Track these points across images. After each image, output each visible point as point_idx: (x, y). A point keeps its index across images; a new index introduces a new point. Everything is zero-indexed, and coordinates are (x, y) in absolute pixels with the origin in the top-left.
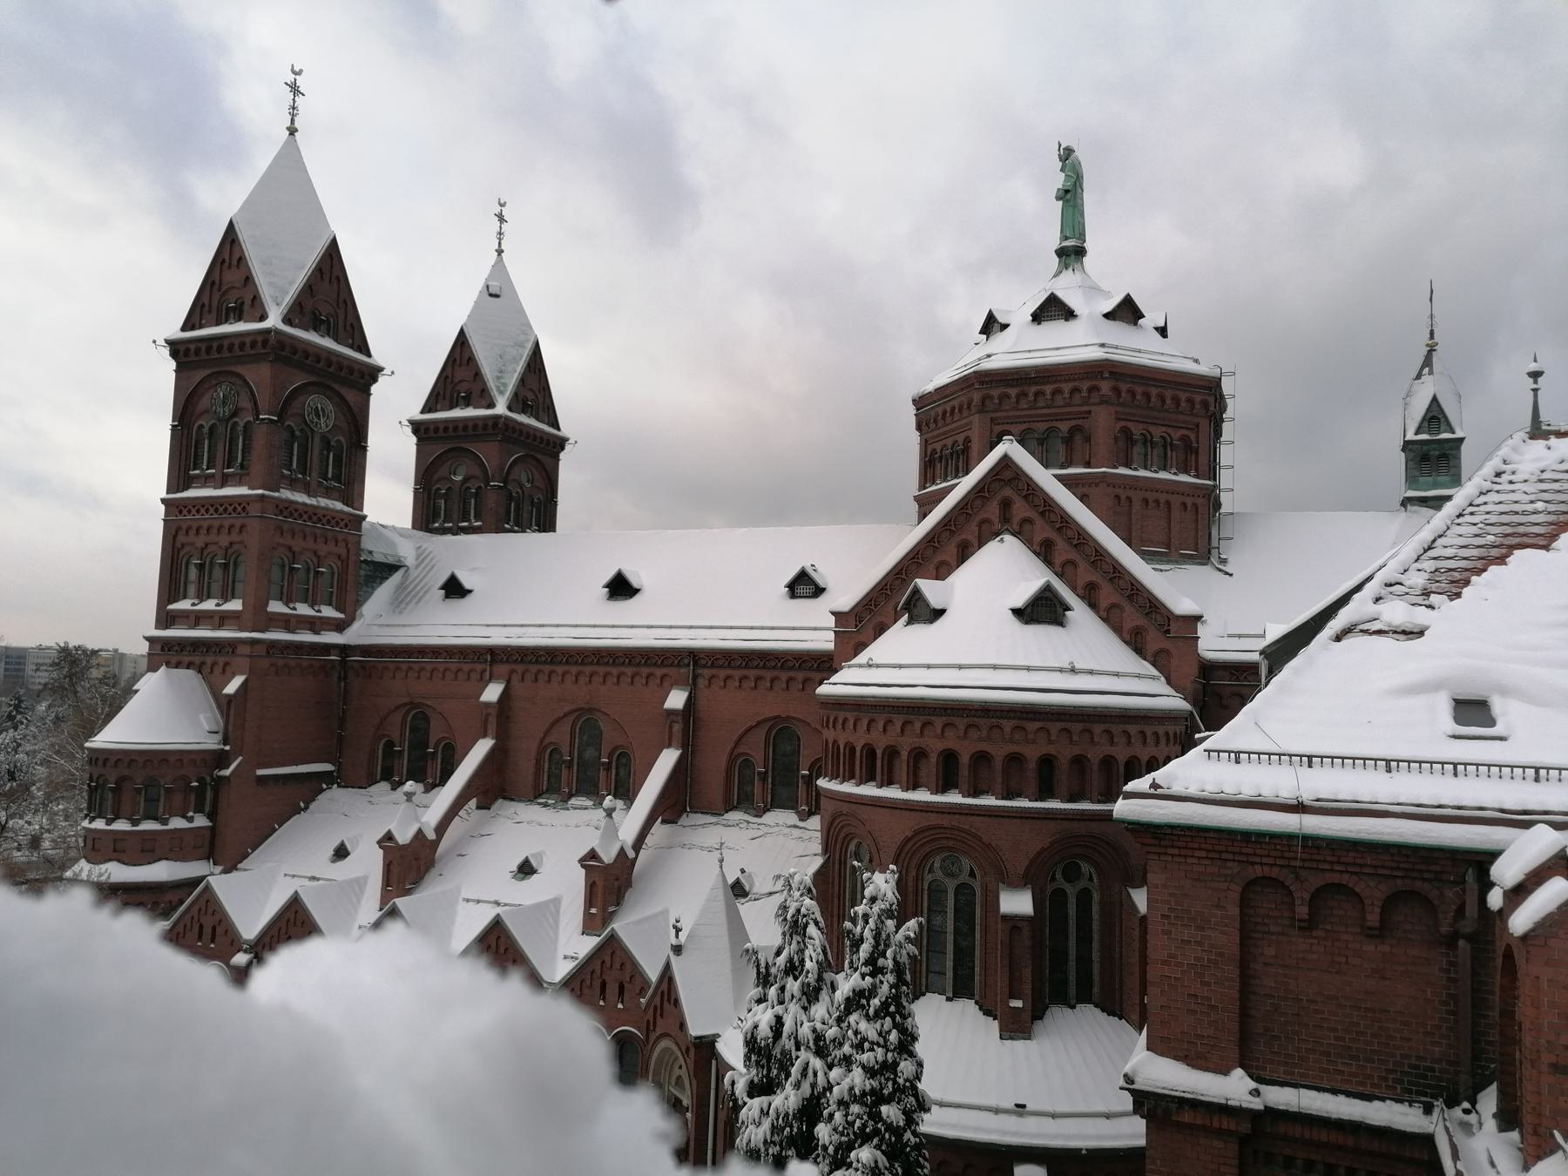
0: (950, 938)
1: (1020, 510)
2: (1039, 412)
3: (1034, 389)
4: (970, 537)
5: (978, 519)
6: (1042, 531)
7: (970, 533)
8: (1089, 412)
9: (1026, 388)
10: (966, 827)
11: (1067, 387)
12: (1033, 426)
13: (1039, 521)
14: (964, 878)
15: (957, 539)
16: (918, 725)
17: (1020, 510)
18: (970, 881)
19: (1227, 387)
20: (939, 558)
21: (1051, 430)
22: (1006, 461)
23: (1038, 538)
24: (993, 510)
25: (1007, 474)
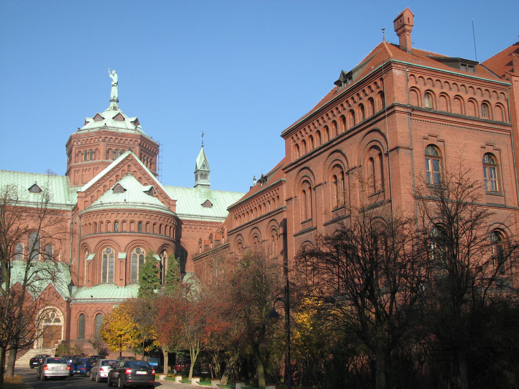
0: (138, 268)
1: (133, 168)
2: (121, 145)
3: (120, 138)
4: (120, 174)
5: (122, 169)
6: (139, 175)
7: (119, 173)
8: (134, 147)
9: (117, 137)
10: (145, 240)
11: (129, 139)
12: (118, 148)
13: (138, 172)
14: (141, 254)
15: (116, 174)
16: (133, 214)
17: (133, 168)
18: (142, 254)
19: (160, 148)
20: (110, 179)
21: (116, 150)
22: (129, 156)
23: (138, 176)
24: (126, 168)
25: (130, 158)
